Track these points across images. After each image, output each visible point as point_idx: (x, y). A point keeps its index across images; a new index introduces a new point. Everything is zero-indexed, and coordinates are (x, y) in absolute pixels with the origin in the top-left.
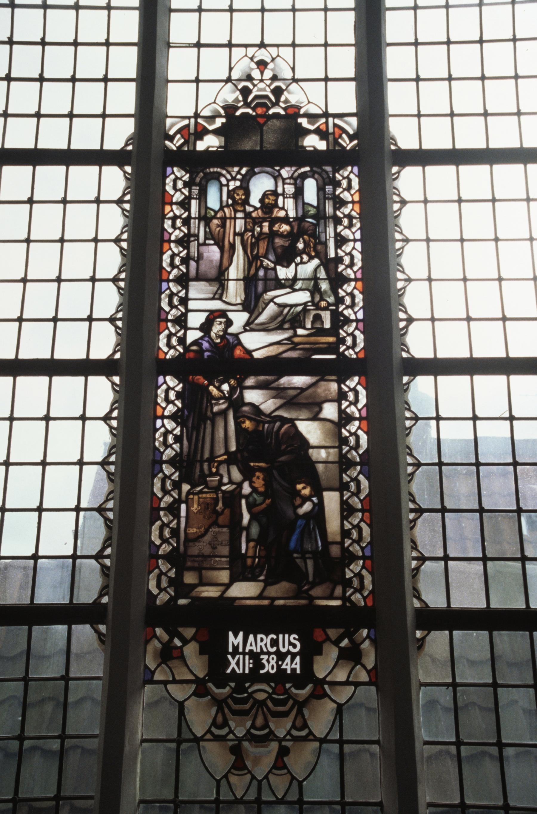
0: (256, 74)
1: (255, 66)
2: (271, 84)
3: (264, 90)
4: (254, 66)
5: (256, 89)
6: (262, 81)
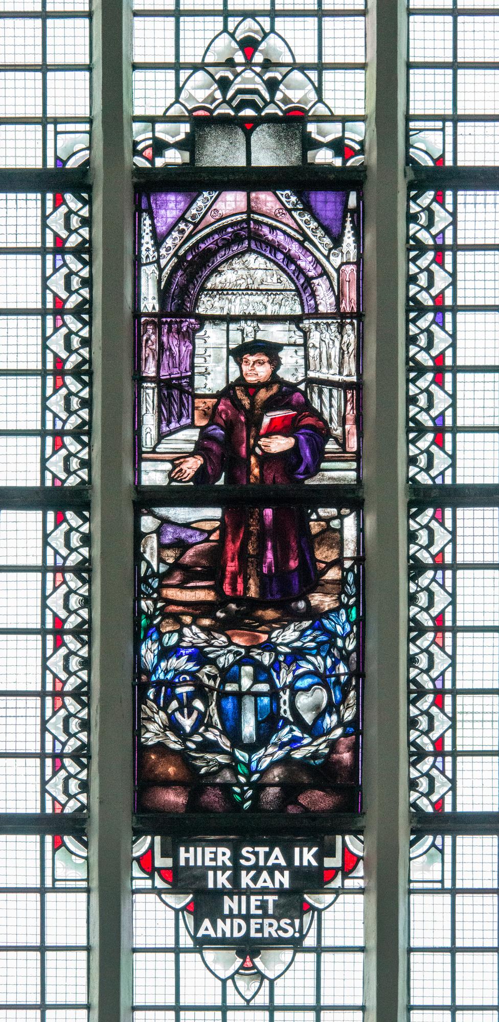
0: (239, 58)
1: (237, 47)
3: (252, 81)
4: (234, 45)
5: (239, 79)
6: (249, 64)
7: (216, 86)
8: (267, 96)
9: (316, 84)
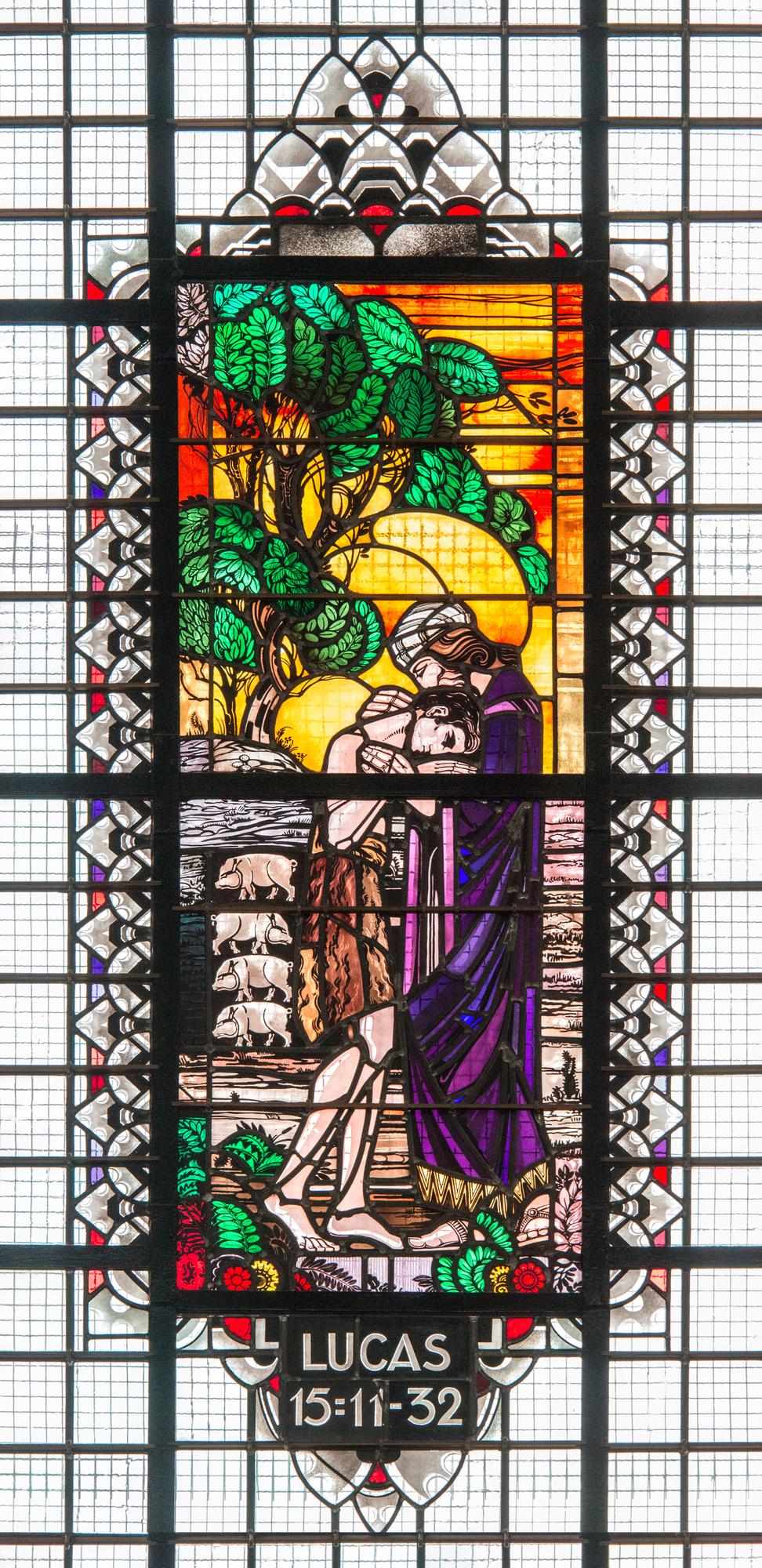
0: (360, 106)
2: (404, 134)
3: (384, 153)
4: (351, 81)
6: (377, 122)
7: (316, 158)
8: (412, 184)
9: (499, 154)
